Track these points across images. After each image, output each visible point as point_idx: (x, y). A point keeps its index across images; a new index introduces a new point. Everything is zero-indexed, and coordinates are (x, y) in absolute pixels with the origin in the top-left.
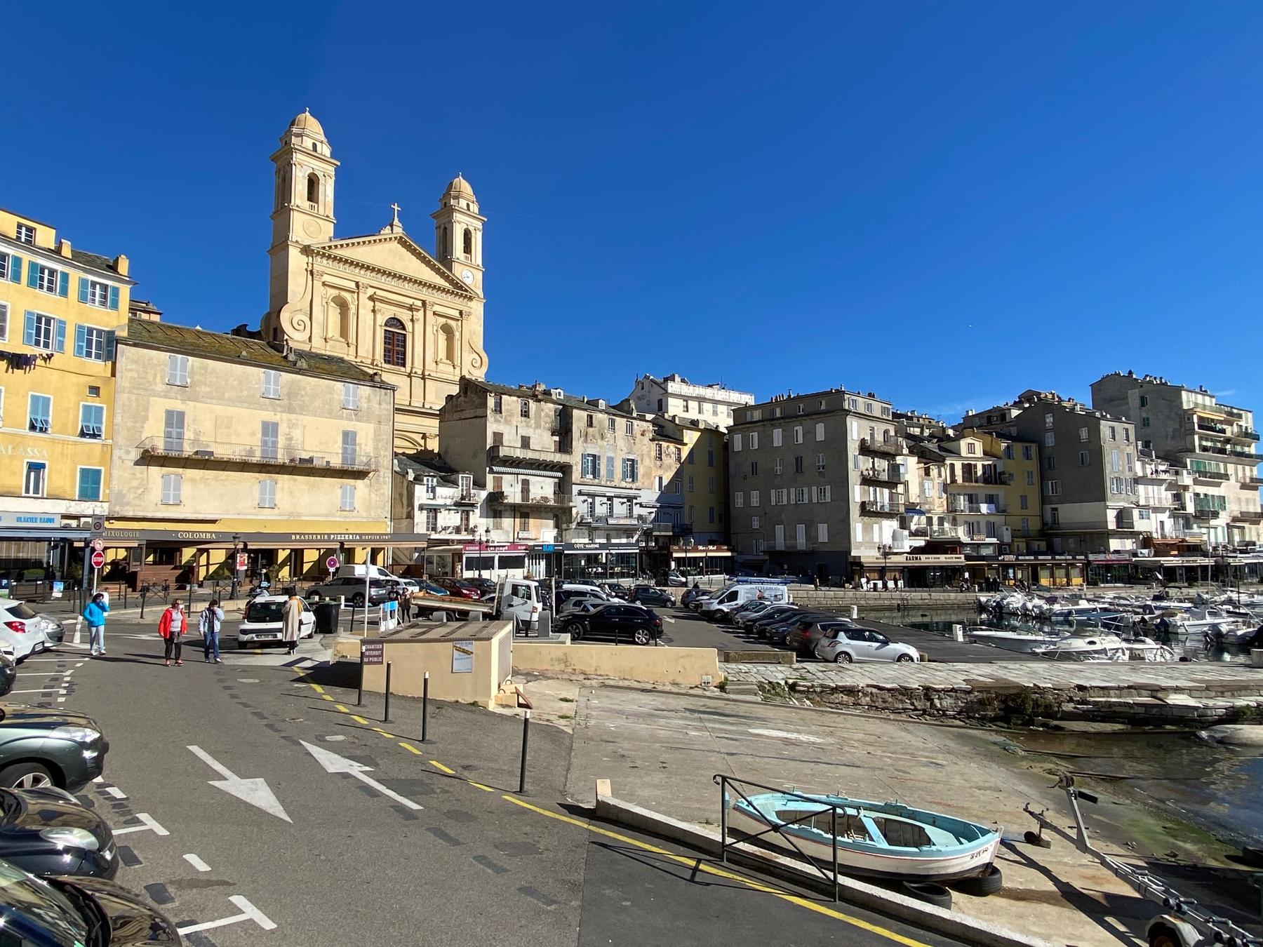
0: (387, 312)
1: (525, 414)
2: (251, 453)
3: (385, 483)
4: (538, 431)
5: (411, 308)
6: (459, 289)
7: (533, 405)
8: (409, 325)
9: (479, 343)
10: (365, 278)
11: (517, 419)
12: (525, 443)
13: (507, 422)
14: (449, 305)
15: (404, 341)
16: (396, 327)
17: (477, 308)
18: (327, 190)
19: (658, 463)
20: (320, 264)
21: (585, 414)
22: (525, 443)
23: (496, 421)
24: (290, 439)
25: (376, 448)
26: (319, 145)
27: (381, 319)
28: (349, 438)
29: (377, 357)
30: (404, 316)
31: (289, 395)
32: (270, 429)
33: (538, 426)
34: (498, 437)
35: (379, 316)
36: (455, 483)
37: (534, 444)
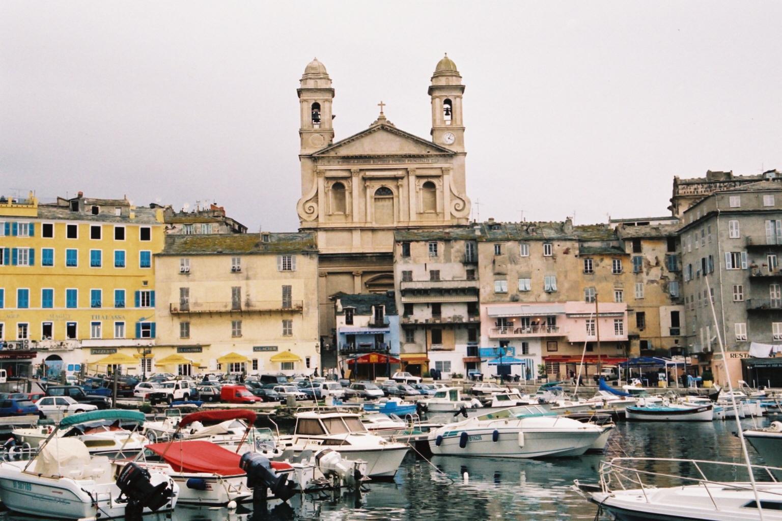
2: (226, 306)
4: (448, 265)
5: (396, 179)
7: (441, 247)
10: (355, 167)
12: (435, 275)
19: (588, 276)
20: (321, 167)
21: (491, 247)
22: (435, 275)
23: (406, 262)
24: (248, 295)
25: (306, 295)
28: (287, 291)
30: (391, 185)
31: (247, 269)
32: (236, 292)
33: (448, 260)
34: (407, 276)
35: (368, 190)
36: (370, 312)
37: (442, 276)
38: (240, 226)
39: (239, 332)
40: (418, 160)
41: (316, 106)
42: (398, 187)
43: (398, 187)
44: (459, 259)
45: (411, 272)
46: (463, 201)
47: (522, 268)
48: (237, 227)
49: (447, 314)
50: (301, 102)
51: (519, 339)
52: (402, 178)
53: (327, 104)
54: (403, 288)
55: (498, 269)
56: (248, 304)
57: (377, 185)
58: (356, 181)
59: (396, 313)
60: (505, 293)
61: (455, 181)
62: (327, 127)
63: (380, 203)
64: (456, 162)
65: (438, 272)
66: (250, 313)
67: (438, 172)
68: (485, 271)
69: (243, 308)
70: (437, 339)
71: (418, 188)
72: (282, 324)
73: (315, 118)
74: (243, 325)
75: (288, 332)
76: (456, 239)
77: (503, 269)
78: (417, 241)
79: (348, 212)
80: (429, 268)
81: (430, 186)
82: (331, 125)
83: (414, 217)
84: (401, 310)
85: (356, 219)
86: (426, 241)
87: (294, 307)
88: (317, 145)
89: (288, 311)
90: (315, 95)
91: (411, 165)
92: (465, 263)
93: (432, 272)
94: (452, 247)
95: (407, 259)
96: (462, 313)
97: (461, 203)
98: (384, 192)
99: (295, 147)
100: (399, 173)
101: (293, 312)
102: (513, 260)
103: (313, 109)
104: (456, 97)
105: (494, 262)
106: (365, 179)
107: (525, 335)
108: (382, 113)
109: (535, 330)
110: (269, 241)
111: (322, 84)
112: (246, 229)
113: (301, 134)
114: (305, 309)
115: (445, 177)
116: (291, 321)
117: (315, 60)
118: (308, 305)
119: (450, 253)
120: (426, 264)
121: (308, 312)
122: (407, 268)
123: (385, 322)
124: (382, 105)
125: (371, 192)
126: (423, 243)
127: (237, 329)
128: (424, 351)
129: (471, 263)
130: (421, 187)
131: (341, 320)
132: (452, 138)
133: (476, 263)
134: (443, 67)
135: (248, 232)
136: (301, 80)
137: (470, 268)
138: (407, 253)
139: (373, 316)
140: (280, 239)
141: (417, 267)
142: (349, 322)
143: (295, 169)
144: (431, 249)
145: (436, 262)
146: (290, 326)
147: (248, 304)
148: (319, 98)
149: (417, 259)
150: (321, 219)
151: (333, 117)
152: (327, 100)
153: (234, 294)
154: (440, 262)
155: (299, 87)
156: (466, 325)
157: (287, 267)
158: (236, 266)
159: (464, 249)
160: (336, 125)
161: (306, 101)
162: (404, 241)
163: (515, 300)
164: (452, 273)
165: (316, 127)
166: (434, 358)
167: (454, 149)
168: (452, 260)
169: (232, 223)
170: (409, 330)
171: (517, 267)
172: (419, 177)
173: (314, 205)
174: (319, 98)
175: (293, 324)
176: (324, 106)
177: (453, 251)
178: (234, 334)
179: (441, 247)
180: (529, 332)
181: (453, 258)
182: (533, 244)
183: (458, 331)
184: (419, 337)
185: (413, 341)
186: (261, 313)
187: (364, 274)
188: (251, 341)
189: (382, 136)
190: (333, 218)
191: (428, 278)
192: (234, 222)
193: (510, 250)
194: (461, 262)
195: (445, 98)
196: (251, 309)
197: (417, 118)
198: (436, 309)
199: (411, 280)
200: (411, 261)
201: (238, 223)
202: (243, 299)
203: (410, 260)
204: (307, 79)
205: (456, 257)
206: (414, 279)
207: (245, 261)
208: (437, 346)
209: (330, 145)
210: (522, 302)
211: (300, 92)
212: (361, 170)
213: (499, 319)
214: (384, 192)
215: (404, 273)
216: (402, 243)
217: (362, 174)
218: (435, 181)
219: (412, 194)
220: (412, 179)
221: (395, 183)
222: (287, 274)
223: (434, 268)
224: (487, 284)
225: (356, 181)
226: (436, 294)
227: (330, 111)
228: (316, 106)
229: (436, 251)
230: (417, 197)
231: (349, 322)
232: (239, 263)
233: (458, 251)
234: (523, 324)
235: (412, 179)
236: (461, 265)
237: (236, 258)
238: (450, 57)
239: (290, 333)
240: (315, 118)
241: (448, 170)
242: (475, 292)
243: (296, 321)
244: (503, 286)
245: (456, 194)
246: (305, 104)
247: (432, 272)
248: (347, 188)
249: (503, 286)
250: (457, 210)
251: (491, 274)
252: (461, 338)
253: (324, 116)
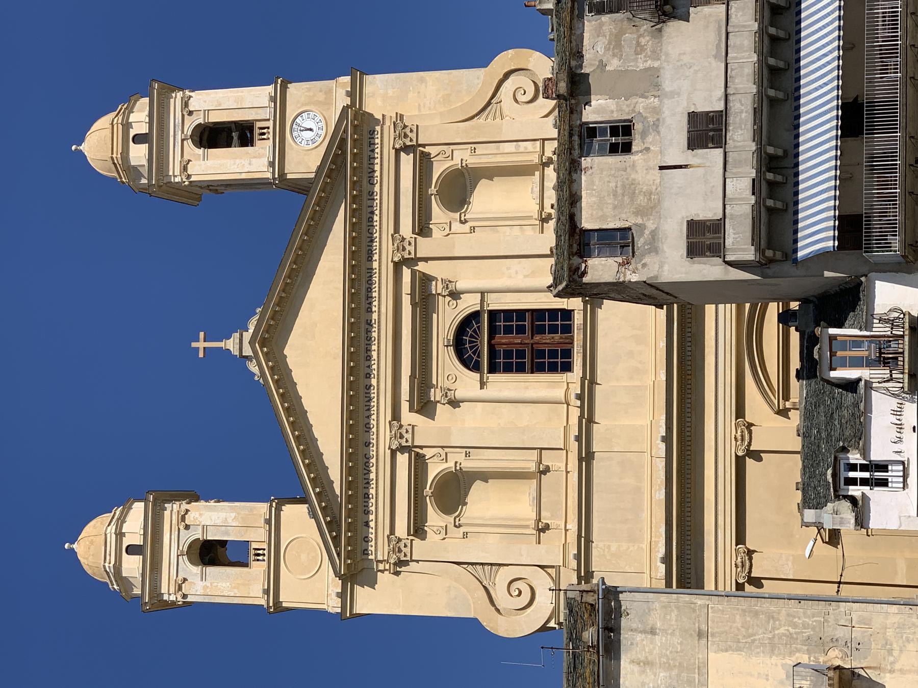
0: (446, 365)
1: (620, 137)
3: (866, 622)
5: (425, 302)
6: (355, 138)
7: (599, 109)
8: (470, 303)
9: (472, 82)
10: (382, 437)
11: (639, 165)
12: (706, 130)
13: (652, 207)
14: (394, 183)
15: (508, 314)
16: (477, 333)
17: (385, 94)
18: (215, 518)
20: (379, 549)
22: (706, 130)
23: (654, 248)
25: (772, 647)
26: (126, 542)
27: (466, 382)
29: (559, 393)
33: (651, 81)
35: (459, 395)
42: (455, 295)
45: (695, 227)
46: (507, 75)
54: (749, 254)
71: (457, 226)
80: (677, 152)
94: (602, 65)
95: (640, 242)
114: (835, 658)
118: (822, 644)
119: (620, 74)
120: (661, 168)
121: (852, 647)
145: (656, 125)
149: (641, 200)
154: (656, 111)
162: (571, 254)
168: (649, 63)
172: (423, 228)
177: (614, 64)
179: (599, 109)
195: (189, 144)
200: (651, 225)
203: (642, 227)
205: (639, 49)
212: (396, 415)
215: (694, 251)
216: (576, 260)
220: (425, 247)
221: (443, 303)
223: (676, 131)
233: (616, 44)
235: (425, 247)
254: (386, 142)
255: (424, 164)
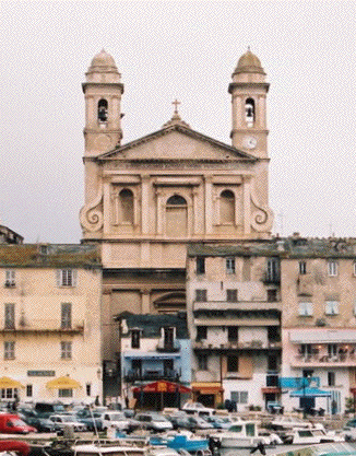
5: (190, 186)
7: (240, 263)
10: (145, 172)
11: (223, 277)
12: (232, 295)
13: (210, 280)
20: (107, 171)
22: (232, 295)
23: (200, 280)
30: (184, 193)
31: (22, 285)
32: (10, 309)
33: (247, 278)
34: (201, 295)
36: (159, 335)
37: (240, 296)
38: (16, 235)
39: (12, 354)
40: (215, 166)
41: (103, 103)
42: (192, 196)
43: (192, 196)
44: (259, 277)
45: (205, 291)
47: (329, 289)
48: (11, 236)
49: (246, 338)
50: (86, 98)
51: (325, 368)
52: (197, 185)
53: (115, 101)
55: (302, 290)
56: (22, 323)
57: (169, 193)
58: (146, 189)
59: (188, 337)
60: (310, 317)
61: (257, 191)
62: (115, 126)
63: (173, 213)
64: (257, 169)
65: (235, 291)
66: (25, 333)
67: (238, 180)
68: (288, 291)
69: (17, 327)
70: (233, 367)
72: (59, 346)
73: (102, 117)
74: (16, 346)
75: (66, 355)
76: (256, 256)
77: (308, 290)
78: (213, 257)
79: (136, 222)
80: (226, 287)
81: (228, 195)
82: (119, 124)
83: (210, 230)
84: (193, 334)
85: (145, 230)
86: (223, 257)
87: (73, 327)
88: (104, 147)
89: (67, 332)
90: (102, 89)
91: (207, 171)
92: (266, 282)
93: (229, 292)
96: (262, 338)
97: (263, 216)
98: (177, 200)
99: (79, 149)
100: (195, 180)
101: (73, 333)
102: (320, 280)
103: (99, 106)
104: (259, 96)
105: (298, 281)
106: (156, 186)
107: (331, 364)
108: (176, 112)
109: (343, 359)
110: (48, 253)
111: (110, 79)
112: (22, 239)
113: (85, 133)
114: (86, 330)
115: (246, 186)
116: (70, 343)
117: (103, 51)
121: (89, 335)
122: (201, 286)
123: (175, 346)
124: (176, 103)
125: (162, 201)
126: (219, 258)
127: (9, 351)
128: (219, 379)
129: (273, 282)
130: (219, 196)
131: (126, 343)
132: (255, 142)
133: (278, 283)
134: (245, 63)
135: (25, 242)
136: (87, 74)
137: (271, 287)
138: (201, 270)
139: (162, 339)
140: (60, 251)
141: (212, 286)
142: (136, 345)
143: (78, 173)
144: (228, 265)
146: (69, 348)
147: (22, 323)
148: (106, 94)
150: (106, 230)
151: (122, 116)
152: (114, 97)
153: (7, 312)
155: (85, 81)
156: (266, 352)
157: (68, 282)
158: (10, 280)
159: (265, 267)
160: (125, 125)
161: (92, 97)
163: (321, 324)
164: (252, 293)
165: (103, 126)
166: (229, 388)
167: (256, 154)
169: (6, 232)
170: (202, 356)
171: (325, 288)
173: (99, 214)
174: (106, 94)
175: (73, 347)
176: (112, 104)
177: (253, 268)
178: (6, 355)
179: (240, 263)
180: (336, 361)
181: (252, 276)
182: (342, 262)
183: (257, 359)
184: (213, 364)
185: (206, 369)
186: (37, 333)
187: (154, 292)
188: (26, 364)
189: (176, 137)
190: (119, 228)
191: (224, 298)
192: (10, 230)
193: (316, 269)
194: (261, 280)
196: (26, 328)
197: (216, 118)
198: (233, 333)
199: (205, 300)
201: (13, 233)
202: (18, 317)
204: (92, 73)
206: (209, 299)
207: (20, 276)
208: (233, 375)
209: (117, 147)
210: (330, 327)
211: (85, 87)
213: (303, 346)
214: (177, 200)
215: (198, 291)
217: (153, 180)
218: (234, 190)
219: (209, 204)
220: (209, 187)
222: (67, 290)
224: (290, 306)
225: (146, 189)
226: (233, 317)
227: (119, 108)
228: (103, 103)
229: (234, 268)
230: (214, 207)
231: (136, 345)
232: (13, 276)
234: (329, 352)
235: (209, 187)
236: (261, 284)
237: (10, 271)
238: (254, 52)
239: (70, 356)
240: (102, 117)
241: (249, 178)
242: (277, 314)
243: (77, 344)
244: (308, 308)
245: (257, 204)
246: (91, 100)
247: (229, 292)
248: (135, 195)
249: (308, 308)
250: (258, 223)
251: (295, 296)
252: (260, 366)
253: (111, 114)
254: (243, 171)
255: (238, 185)
